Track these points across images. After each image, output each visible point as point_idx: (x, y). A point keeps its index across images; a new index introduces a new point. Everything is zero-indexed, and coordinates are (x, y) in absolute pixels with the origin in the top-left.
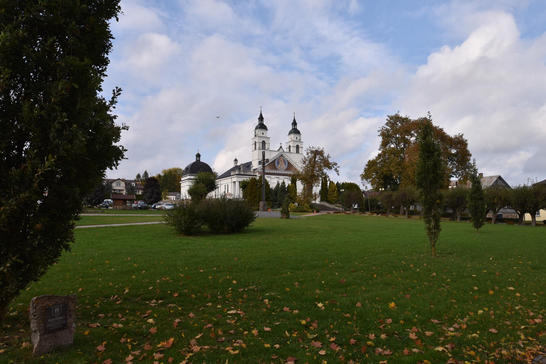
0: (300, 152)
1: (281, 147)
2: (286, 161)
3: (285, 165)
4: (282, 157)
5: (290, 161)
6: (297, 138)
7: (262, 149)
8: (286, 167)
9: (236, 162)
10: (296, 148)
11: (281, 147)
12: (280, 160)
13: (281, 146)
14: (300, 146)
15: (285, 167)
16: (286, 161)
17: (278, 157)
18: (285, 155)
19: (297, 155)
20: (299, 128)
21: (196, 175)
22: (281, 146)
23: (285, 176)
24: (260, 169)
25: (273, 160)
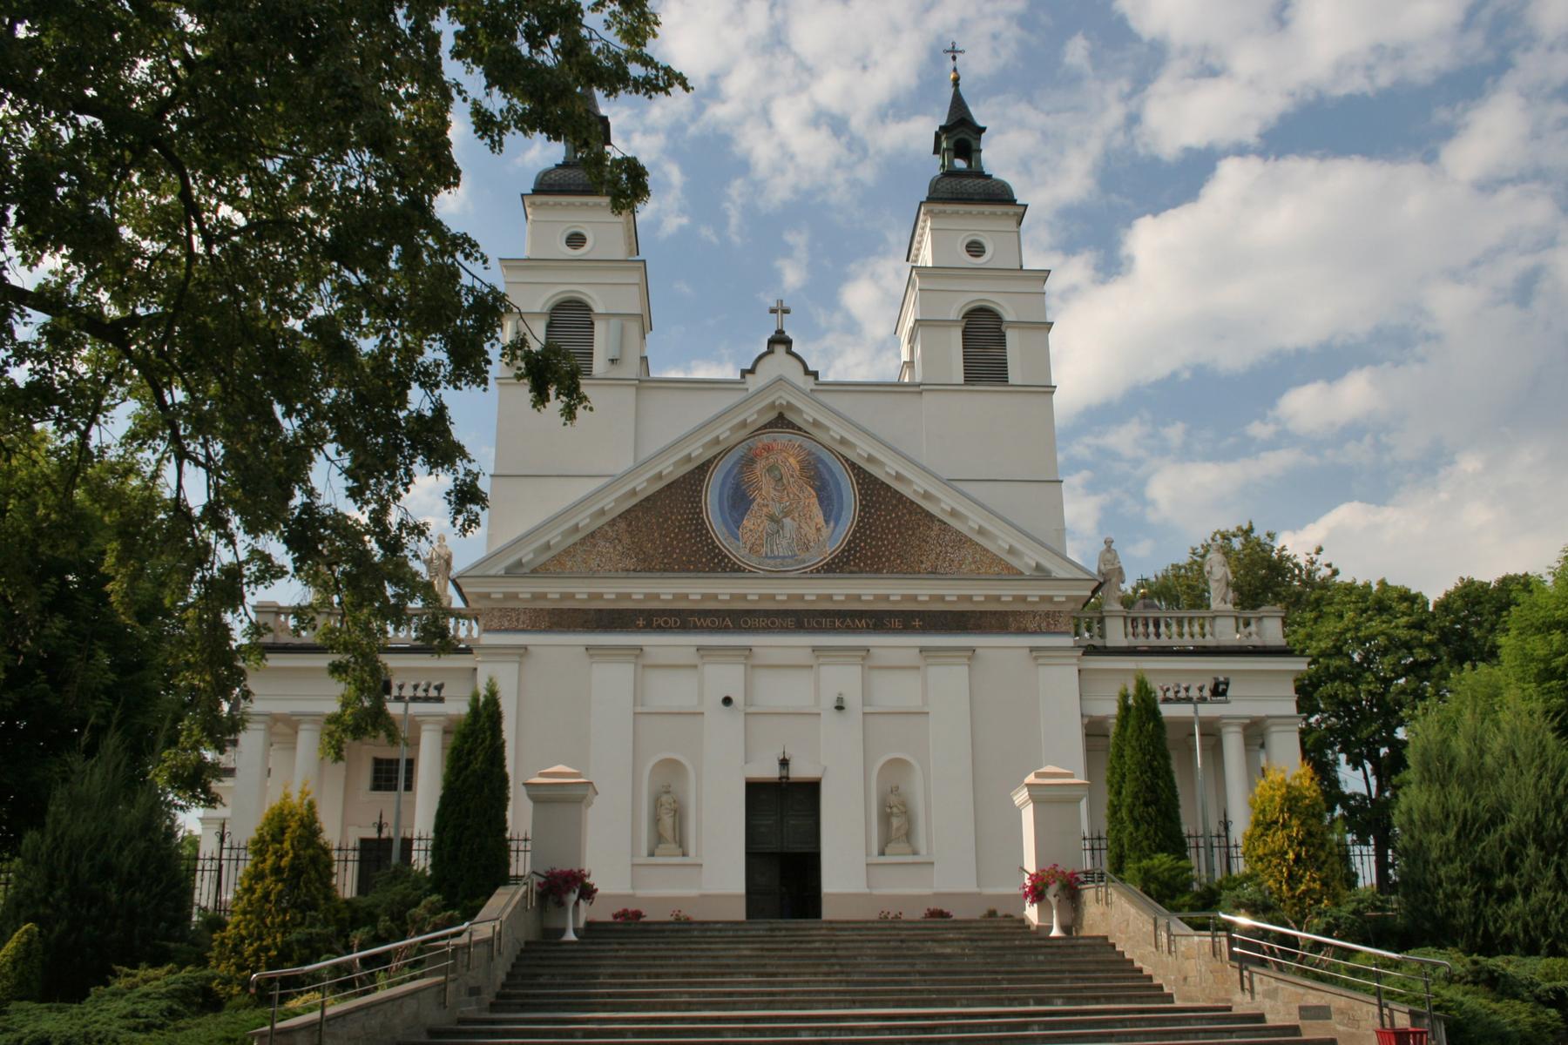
1: (780, 340)
2: (838, 468)
4: (782, 438)
5: (887, 468)
6: (975, 249)
11: (780, 340)
12: (760, 466)
13: (780, 332)
14: (1008, 315)
15: (833, 537)
16: (838, 468)
18: (808, 412)
19: (986, 402)
20: (995, 157)
22: (780, 332)
24: (499, 569)
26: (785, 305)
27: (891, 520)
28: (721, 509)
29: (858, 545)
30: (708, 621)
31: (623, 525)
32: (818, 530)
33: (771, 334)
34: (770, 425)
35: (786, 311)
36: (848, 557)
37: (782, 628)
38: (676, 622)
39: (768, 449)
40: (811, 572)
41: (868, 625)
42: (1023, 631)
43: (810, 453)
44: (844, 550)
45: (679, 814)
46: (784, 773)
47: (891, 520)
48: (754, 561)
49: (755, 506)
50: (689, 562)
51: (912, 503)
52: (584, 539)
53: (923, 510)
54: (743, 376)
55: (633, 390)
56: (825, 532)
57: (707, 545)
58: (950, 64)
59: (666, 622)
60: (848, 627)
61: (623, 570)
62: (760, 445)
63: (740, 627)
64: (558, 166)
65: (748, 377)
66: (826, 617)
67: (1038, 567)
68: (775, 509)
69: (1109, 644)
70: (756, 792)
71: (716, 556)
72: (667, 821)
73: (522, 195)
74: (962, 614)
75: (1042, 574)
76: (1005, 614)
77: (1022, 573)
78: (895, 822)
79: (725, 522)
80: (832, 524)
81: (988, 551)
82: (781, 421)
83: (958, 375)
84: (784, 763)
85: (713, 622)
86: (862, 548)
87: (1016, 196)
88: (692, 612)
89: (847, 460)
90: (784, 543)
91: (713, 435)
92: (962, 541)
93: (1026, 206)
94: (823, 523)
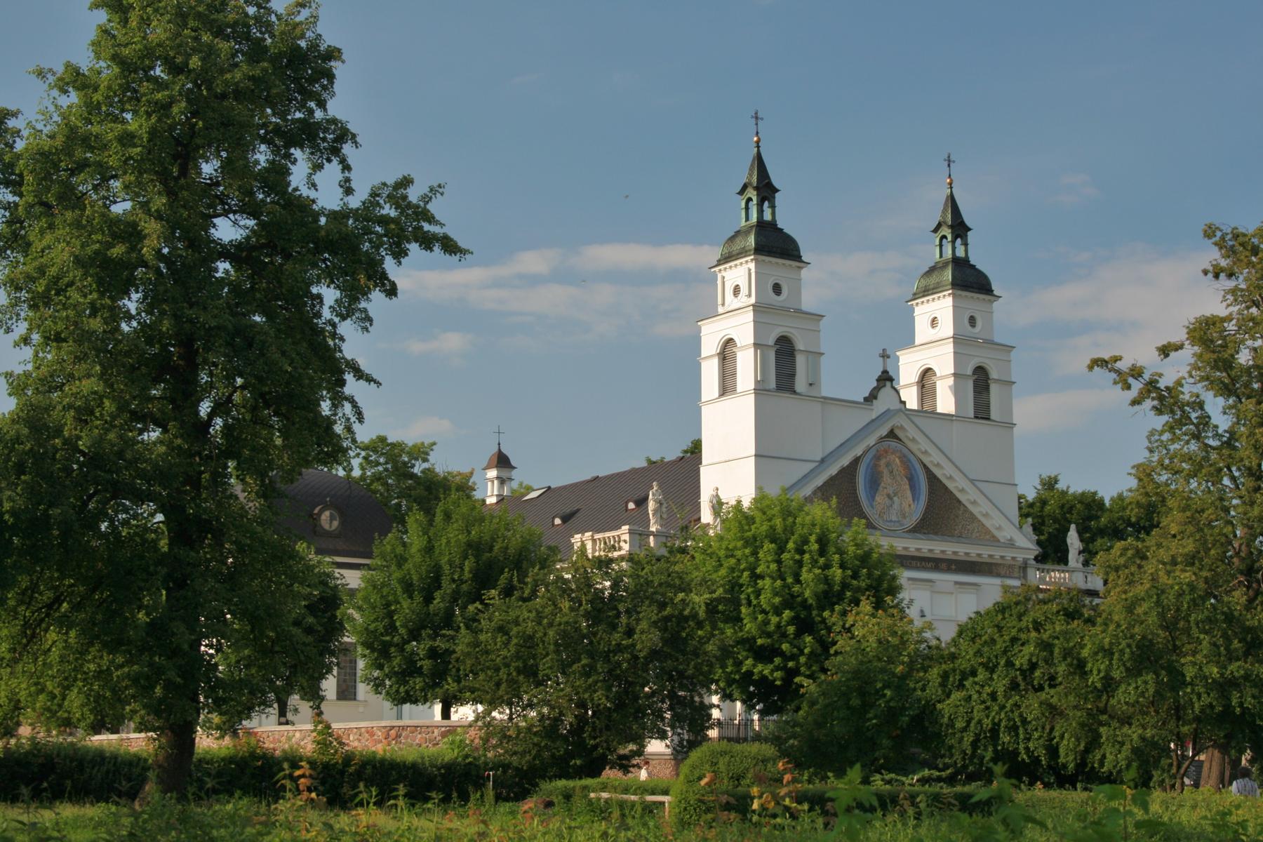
0: (994, 414)
3: (915, 497)
4: (893, 444)
5: (944, 472)
8: (915, 510)
9: (505, 474)
12: (883, 462)
13: (885, 372)
17: (871, 440)
18: (912, 432)
19: (982, 426)
21: (368, 567)
22: (885, 372)
25: (845, 461)
35: (888, 357)
42: (998, 575)
49: (881, 489)
67: (1011, 540)
68: (890, 491)
77: (999, 541)
87: (993, 288)
92: (973, 518)
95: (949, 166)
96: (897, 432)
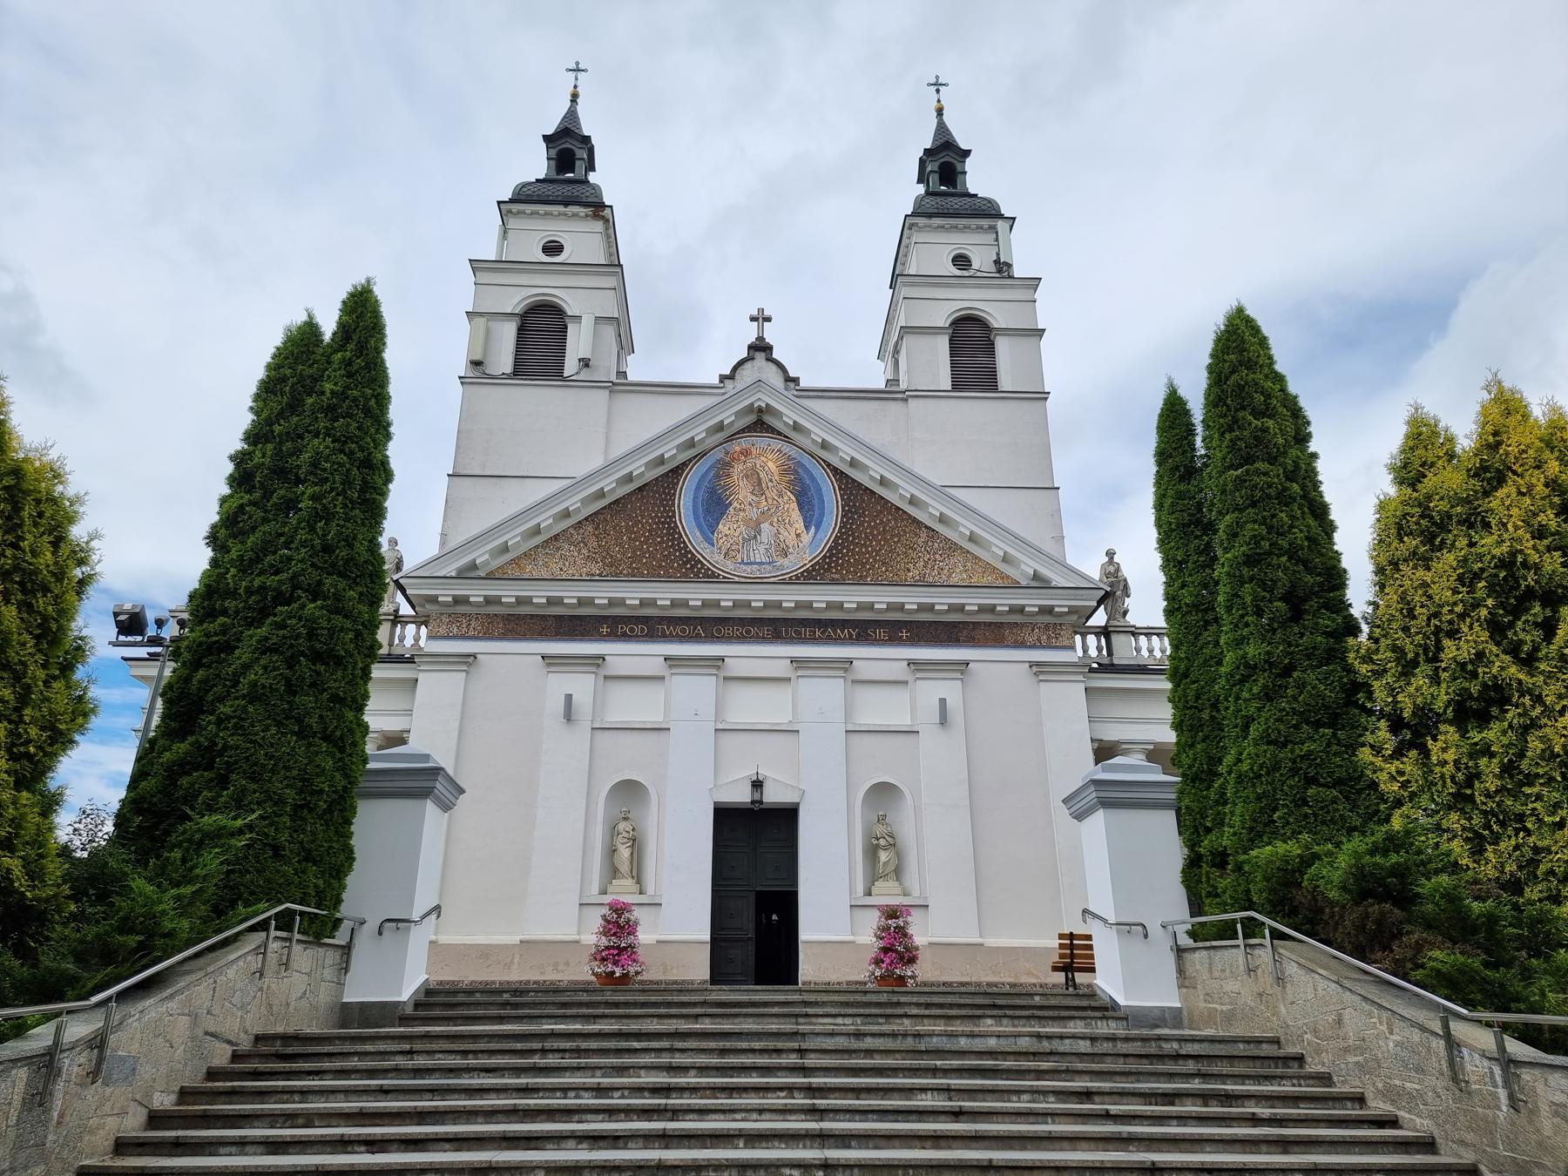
1: (760, 348)
2: (820, 473)
4: (761, 442)
6: (961, 261)
7: (517, 373)
10: (943, 344)
11: (760, 348)
12: (738, 469)
13: (761, 338)
18: (790, 415)
19: (974, 410)
20: (977, 180)
22: (761, 338)
23: (813, 640)
24: (451, 570)
26: (766, 313)
27: (875, 527)
28: (696, 517)
29: (840, 551)
30: (678, 629)
31: (590, 528)
32: (798, 536)
33: (752, 339)
34: (749, 429)
35: (768, 319)
36: (829, 564)
37: (758, 637)
38: (642, 630)
39: (746, 453)
40: (790, 578)
41: (851, 636)
42: (1021, 645)
43: (790, 458)
44: (825, 556)
45: (636, 843)
46: (757, 797)
47: (875, 527)
48: (730, 566)
50: (660, 566)
51: (898, 508)
52: (547, 541)
53: (910, 516)
54: (721, 381)
55: (607, 392)
56: (806, 538)
57: (681, 549)
58: (936, 97)
59: (632, 630)
60: (829, 637)
61: (587, 575)
62: (738, 449)
63: (713, 636)
64: (538, 181)
65: (727, 382)
66: (805, 627)
69: (1116, 662)
70: (725, 817)
71: (689, 561)
72: (624, 852)
73: (499, 203)
74: (954, 625)
75: (1040, 582)
76: (1000, 625)
77: (1018, 583)
78: (883, 856)
79: (699, 526)
80: (813, 530)
81: (980, 559)
82: (760, 423)
83: (946, 383)
84: (757, 785)
85: (683, 631)
86: (844, 555)
88: (661, 620)
89: (829, 465)
90: (762, 548)
91: (688, 436)
92: (952, 547)
93: (1014, 219)
94: (803, 528)
95: (938, 91)
96: (770, 420)
